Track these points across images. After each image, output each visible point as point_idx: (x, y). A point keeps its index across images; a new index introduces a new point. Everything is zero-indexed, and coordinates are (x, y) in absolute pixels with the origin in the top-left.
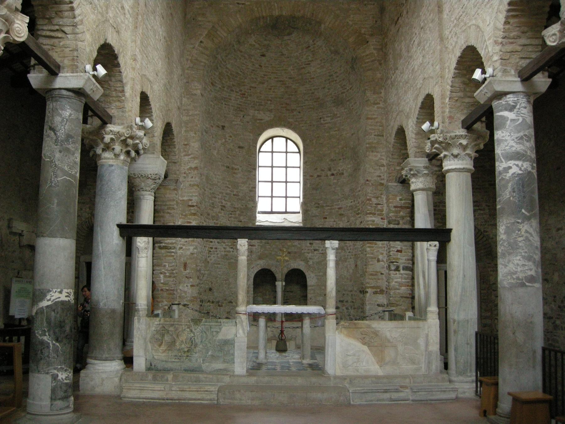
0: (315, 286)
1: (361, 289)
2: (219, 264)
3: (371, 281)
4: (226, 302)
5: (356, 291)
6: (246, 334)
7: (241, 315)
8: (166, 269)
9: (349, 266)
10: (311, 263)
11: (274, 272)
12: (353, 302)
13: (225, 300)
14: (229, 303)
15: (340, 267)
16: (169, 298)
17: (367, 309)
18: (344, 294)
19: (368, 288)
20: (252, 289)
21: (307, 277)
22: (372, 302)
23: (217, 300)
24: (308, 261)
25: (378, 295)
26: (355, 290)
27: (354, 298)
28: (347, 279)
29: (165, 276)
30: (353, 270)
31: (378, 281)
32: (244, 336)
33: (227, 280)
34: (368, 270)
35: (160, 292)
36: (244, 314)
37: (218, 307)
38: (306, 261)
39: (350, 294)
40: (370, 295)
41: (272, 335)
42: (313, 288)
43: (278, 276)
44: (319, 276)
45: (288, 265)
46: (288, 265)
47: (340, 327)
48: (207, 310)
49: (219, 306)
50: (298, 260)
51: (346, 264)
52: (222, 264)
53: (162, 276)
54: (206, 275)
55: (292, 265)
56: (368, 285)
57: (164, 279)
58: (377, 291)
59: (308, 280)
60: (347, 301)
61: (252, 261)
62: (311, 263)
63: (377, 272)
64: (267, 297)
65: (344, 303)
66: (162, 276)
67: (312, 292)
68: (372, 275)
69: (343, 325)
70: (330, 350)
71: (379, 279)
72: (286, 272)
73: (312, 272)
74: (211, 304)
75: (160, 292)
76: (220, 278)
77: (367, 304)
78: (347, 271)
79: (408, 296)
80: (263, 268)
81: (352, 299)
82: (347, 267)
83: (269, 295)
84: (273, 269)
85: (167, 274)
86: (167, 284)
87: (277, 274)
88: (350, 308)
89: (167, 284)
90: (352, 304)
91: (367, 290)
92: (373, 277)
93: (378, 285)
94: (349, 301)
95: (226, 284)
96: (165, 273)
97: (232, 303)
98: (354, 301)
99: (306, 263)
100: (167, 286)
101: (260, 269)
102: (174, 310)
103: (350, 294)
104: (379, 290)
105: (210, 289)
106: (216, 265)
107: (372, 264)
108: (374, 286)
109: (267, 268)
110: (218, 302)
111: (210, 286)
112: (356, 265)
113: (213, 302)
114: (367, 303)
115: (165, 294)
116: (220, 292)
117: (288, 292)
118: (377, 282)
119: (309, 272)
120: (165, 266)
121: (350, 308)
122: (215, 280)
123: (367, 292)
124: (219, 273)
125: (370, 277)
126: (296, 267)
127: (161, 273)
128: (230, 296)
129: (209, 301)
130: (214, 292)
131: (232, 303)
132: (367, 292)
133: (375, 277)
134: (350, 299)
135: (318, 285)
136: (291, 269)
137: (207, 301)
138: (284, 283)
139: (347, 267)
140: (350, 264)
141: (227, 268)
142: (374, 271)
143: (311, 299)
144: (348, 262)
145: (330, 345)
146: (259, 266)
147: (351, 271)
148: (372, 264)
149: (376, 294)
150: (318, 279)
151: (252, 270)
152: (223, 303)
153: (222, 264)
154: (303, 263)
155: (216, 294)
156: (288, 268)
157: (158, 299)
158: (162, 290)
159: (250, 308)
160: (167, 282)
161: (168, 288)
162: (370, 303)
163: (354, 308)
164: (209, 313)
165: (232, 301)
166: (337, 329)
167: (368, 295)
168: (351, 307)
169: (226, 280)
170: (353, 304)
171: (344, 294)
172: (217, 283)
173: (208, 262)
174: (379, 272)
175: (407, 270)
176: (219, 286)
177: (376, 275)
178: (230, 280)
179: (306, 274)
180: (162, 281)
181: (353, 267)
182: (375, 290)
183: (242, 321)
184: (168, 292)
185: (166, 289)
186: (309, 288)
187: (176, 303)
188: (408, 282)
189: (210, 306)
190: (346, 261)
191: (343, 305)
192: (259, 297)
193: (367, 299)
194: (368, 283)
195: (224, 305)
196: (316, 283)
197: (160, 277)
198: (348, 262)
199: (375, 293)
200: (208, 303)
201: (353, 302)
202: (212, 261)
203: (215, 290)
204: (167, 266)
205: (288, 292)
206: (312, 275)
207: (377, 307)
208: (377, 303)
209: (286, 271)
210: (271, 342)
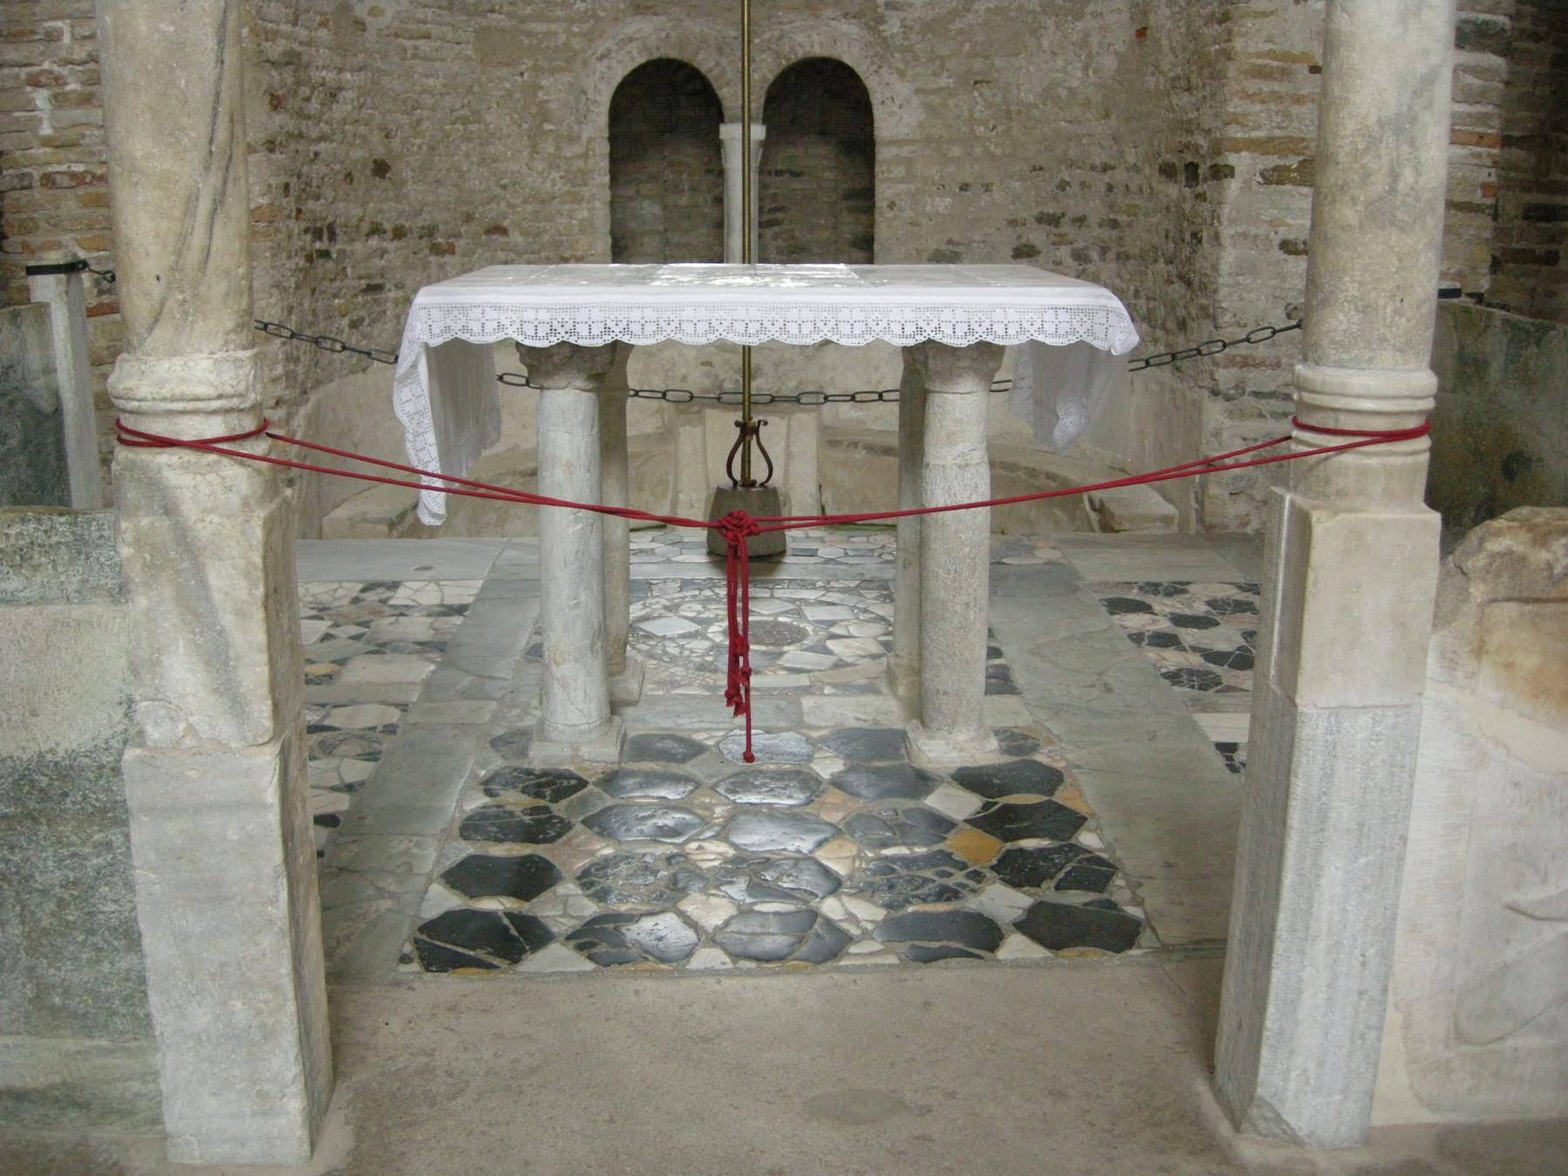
0: (912, 142)
1: (1169, 157)
2: (427, 37)
3: (1258, 107)
4: (474, 227)
5: (1136, 168)
6: (262, 711)
7: (164, 457)
8: (63, 54)
9: (1094, 40)
10: (892, 27)
11: (711, 76)
12: (1114, 224)
13: (468, 218)
14: (488, 232)
15: (1045, 44)
16: (90, 227)
17: (1225, 268)
18: (1063, 185)
19: (1237, 147)
20: (605, 164)
21: (877, 95)
22: (1253, 231)
23: (424, 220)
24: (880, 20)
25: (1288, 187)
26: (1131, 160)
27: (1122, 200)
28: (1087, 104)
29: (59, 100)
30: (1122, 58)
31: (1294, 109)
32: (227, 729)
33: (477, 117)
34: (1238, 44)
35: (38, 194)
36: (203, 446)
37: (432, 259)
38: (871, 22)
39: (1099, 181)
40: (1246, 187)
41: (707, 382)
42: (905, 152)
43: (729, 95)
44: (938, 91)
45: (780, 38)
46: (780, 38)
47: (1478, 591)
48: (369, 277)
49: (436, 249)
50: (829, 13)
51: (1079, 25)
52: (442, 38)
53: (41, 98)
54: (350, 94)
55: (800, 38)
56: (1235, 132)
57: (53, 118)
58: (1288, 168)
59: (878, 112)
60: (1080, 221)
61: (598, 19)
62: (895, 31)
63: (1287, 57)
64: (684, 200)
65: (1066, 228)
66: (41, 98)
67: (899, 172)
68: (1261, 73)
69: (1515, 562)
70: (1335, 871)
71: (1298, 100)
72: (771, 77)
73: (901, 74)
74: (391, 246)
75: (38, 194)
76: (433, 109)
77: (1226, 240)
78: (1086, 68)
79: (1477, 197)
80: (656, 55)
81: (1111, 206)
82: (1084, 43)
83: (694, 189)
84: (705, 63)
85: (73, 86)
86: (74, 145)
87: (728, 84)
88: (1094, 255)
89: (74, 145)
90: (1107, 234)
91: (1232, 159)
92: (1266, 86)
93: (1295, 129)
94: (1093, 219)
95: (467, 138)
96: (59, 81)
97: (503, 231)
98: (1122, 218)
99: (870, 28)
100: (72, 156)
101: (641, 60)
102: (42, 311)
103: (1099, 181)
104: (1293, 161)
105: (381, 168)
106: (409, 44)
107: (1264, 14)
108: (1270, 139)
109: (673, 54)
110: (429, 231)
111: (380, 152)
112: (1142, 33)
113: (399, 233)
114: (1227, 232)
115: (70, 205)
116: (438, 182)
117: (779, 173)
118: (1287, 115)
119: (883, 71)
120: (52, 37)
121: (1094, 255)
122: (405, 119)
123: (1230, 172)
124: (431, 82)
125: (1252, 85)
126: (818, 51)
127: (35, 82)
128: (492, 199)
129: (376, 230)
130: (404, 183)
131: (503, 231)
132: (1230, 172)
133: (1276, 86)
134: (1094, 208)
135: (929, 140)
136: (793, 59)
137: (365, 227)
138: (758, 132)
139: (1084, 43)
140: (1103, 29)
141: (469, 59)
142: (1270, 54)
143: (892, 205)
144: (1095, 15)
145: (1343, 812)
146: (633, 47)
147: (1109, 63)
148: (1264, 14)
149: (1280, 182)
150: (930, 109)
151: (601, 67)
152: (458, 236)
153: (442, 38)
154: (850, 29)
155: (414, 191)
156: (778, 54)
157: (28, 238)
158: (48, 180)
159: (449, 310)
160: (71, 134)
161: (79, 168)
162: (1245, 235)
163: (1122, 257)
164: (378, 288)
165: (506, 223)
166: (1440, 619)
167: (1233, 187)
168: (1104, 250)
169: (465, 121)
170: (1115, 234)
171: (1063, 185)
172: (417, 135)
173: (361, 25)
174: (1304, 57)
175: (1480, 47)
176: (432, 148)
177: (1285, 74)
178: (489, 118)
179: (871, 83)
180: (46, 130)
181: (1122, 36)
182: (1272, 161)
183: (184, 540)
184: (81, 191)
185: (73, 176)
186: (883, 154)
187: (54, 258)
188: (1483, 119)
189: (383, 253)
190: (1079, 16)
191: (1061, 240)
192: (646, 204)
193: (1226, 211)
194: (1235, 120)
195: (460, 244)
196: (921, 125)
197: (29, 107)
198: (1095, 15)
199: (1274, 177)
200: (374, 242)
201: (1114, 224)
202: (382, 22)
203: (407, 174)
204: (67, 39)
205: (779, 173)
206: (902, 89)
207: (1281, 255)
208: (1285, 234)
209: (766, 70)
210: (702, 421)
